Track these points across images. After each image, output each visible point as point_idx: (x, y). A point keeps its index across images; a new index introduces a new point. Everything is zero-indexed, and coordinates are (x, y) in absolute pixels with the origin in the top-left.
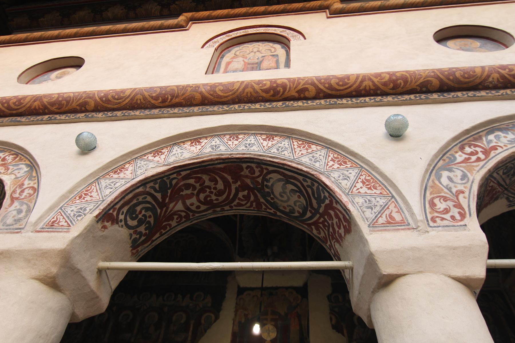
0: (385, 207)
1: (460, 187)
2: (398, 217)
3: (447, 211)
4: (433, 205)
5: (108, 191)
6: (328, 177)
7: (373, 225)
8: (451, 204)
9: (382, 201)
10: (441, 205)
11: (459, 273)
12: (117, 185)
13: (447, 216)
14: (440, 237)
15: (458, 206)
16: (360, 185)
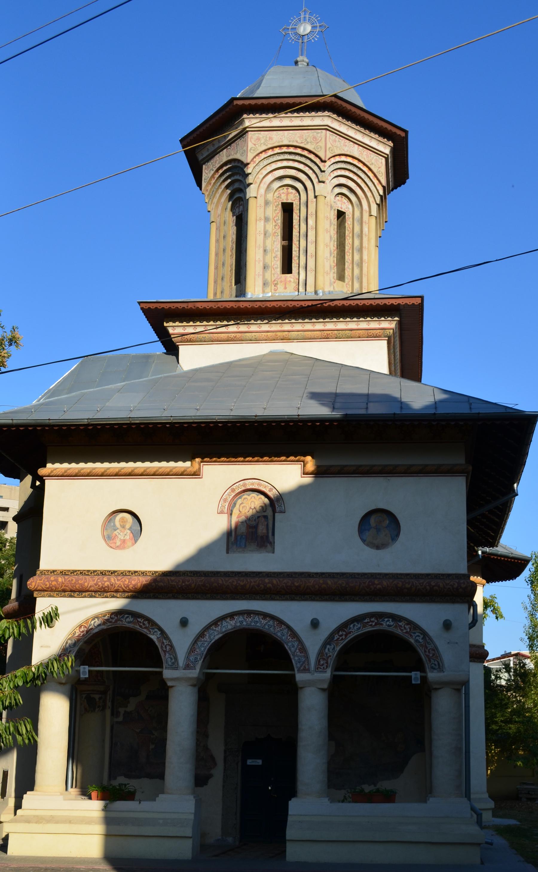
0: (304, 662)
1: (331, 654)
2: (307, 667)
3: (323, 665)
4: (319, 661)
5: (203, 649)
6: (287, 645)
7: (299, 671)
8: (325, 661)
9: (304, 659)
10: (322, 662)
11: (320, 687)
12: (205, 645)
13: (322, 667)
14: (318, 676)
15: (327, 663)
16: (298, 651)
